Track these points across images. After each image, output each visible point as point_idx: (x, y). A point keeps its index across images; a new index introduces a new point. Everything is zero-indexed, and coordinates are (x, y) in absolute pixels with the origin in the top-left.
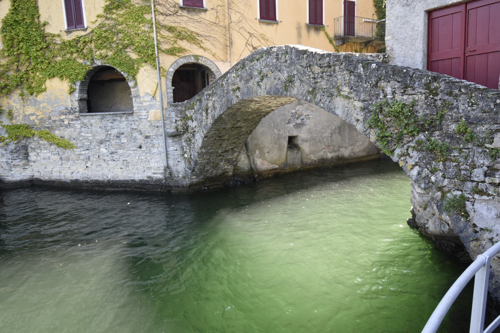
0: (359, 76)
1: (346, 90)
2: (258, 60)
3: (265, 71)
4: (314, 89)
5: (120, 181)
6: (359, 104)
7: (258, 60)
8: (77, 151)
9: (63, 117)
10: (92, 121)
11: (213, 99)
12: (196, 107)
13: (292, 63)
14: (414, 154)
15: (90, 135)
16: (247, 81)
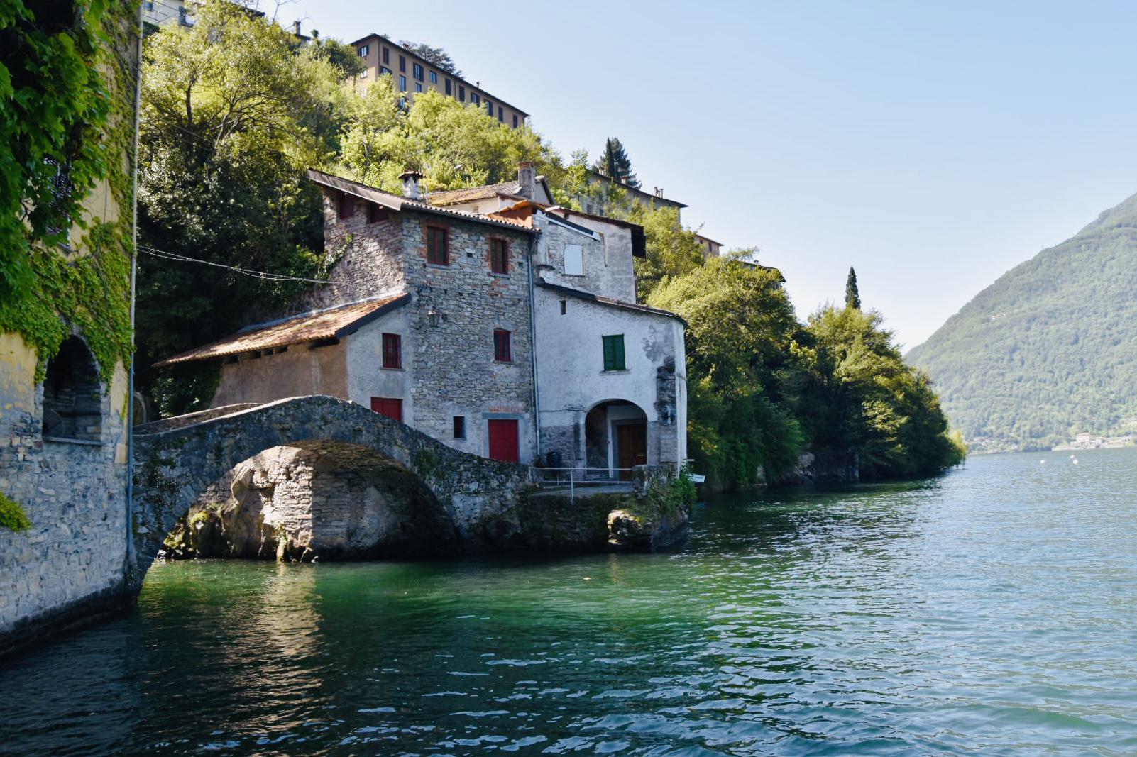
0: (407, 434)
1: (399, 442)
2: (319, 405)
3: (330, 417)
4: (378, 439)
5: (82, 599)
6: (407, 451)
7: (319, 405)
8: (35, 535)
9: (16, 441)
10: (58, 457)
11: (238, 437)
12: (187, 446)
13: (358, 417)
14: (433, 478)
15: (51, 492)
16: (303, 423)
